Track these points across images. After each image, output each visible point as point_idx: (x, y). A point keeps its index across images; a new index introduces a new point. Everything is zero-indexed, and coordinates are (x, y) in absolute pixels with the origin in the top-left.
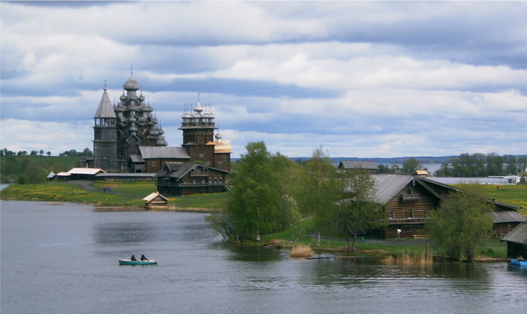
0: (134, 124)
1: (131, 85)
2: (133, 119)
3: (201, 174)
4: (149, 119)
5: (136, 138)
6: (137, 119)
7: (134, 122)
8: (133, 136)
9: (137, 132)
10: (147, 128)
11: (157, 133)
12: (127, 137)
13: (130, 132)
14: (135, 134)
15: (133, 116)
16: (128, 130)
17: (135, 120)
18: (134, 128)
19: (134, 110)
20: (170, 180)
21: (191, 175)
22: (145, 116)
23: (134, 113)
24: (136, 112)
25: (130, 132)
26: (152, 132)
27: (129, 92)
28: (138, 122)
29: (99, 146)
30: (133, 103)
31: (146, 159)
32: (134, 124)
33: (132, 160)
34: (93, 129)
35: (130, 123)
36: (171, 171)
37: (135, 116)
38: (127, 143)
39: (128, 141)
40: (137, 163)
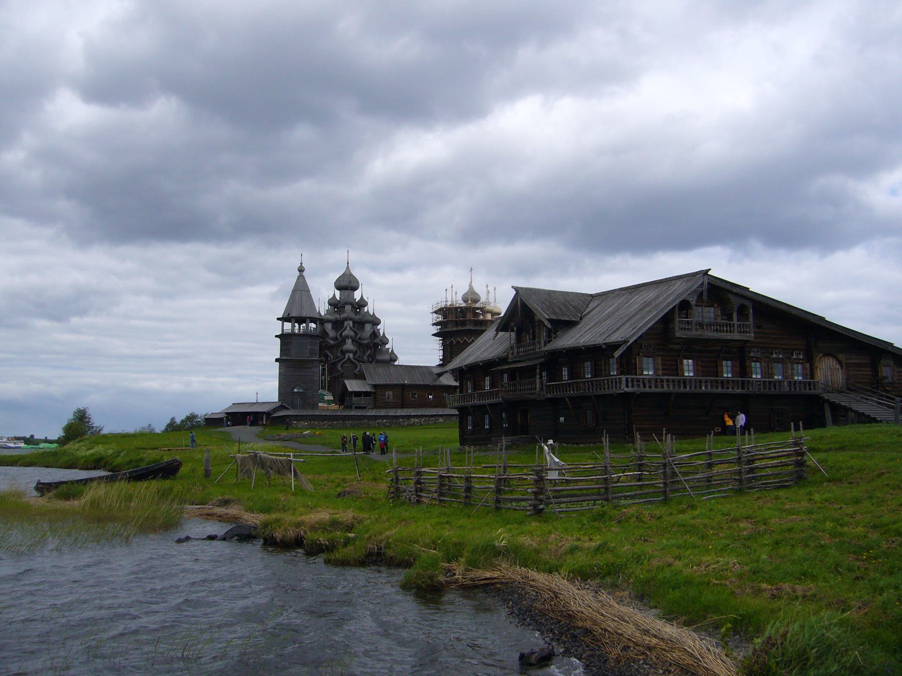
0: (349, 341)
2: (348, 332)
3: (719, 328)
5: (354, 363)
6: (356, 333)
7: (351, 337)
8: (349, 358)
9: (355, 353)
10: (371, 349)
11: (387, 357)
12: (339, 361)
13: (343, 353)
14: (351, 356)
15: (348, 328)
16: (340, 350)
17: (352, 333)
18: (349, 345)
19: (351, 319)
20: (545, 366)
21: (678, 334)
22: (368, 327)
23: (351, 323)
24: (354, 323)
25: (343, 353)
26: (379, 357)
27: (342, 291)
29: (287, 367)
30: (348, 308)
32: (349, 341)
33: (347, 389)
34: (278, 340)
35: (344, 340)
36: (550, 320)
37: (353, 329)
38: (339, 371)
39: (339, 368)
40: (358, 394)
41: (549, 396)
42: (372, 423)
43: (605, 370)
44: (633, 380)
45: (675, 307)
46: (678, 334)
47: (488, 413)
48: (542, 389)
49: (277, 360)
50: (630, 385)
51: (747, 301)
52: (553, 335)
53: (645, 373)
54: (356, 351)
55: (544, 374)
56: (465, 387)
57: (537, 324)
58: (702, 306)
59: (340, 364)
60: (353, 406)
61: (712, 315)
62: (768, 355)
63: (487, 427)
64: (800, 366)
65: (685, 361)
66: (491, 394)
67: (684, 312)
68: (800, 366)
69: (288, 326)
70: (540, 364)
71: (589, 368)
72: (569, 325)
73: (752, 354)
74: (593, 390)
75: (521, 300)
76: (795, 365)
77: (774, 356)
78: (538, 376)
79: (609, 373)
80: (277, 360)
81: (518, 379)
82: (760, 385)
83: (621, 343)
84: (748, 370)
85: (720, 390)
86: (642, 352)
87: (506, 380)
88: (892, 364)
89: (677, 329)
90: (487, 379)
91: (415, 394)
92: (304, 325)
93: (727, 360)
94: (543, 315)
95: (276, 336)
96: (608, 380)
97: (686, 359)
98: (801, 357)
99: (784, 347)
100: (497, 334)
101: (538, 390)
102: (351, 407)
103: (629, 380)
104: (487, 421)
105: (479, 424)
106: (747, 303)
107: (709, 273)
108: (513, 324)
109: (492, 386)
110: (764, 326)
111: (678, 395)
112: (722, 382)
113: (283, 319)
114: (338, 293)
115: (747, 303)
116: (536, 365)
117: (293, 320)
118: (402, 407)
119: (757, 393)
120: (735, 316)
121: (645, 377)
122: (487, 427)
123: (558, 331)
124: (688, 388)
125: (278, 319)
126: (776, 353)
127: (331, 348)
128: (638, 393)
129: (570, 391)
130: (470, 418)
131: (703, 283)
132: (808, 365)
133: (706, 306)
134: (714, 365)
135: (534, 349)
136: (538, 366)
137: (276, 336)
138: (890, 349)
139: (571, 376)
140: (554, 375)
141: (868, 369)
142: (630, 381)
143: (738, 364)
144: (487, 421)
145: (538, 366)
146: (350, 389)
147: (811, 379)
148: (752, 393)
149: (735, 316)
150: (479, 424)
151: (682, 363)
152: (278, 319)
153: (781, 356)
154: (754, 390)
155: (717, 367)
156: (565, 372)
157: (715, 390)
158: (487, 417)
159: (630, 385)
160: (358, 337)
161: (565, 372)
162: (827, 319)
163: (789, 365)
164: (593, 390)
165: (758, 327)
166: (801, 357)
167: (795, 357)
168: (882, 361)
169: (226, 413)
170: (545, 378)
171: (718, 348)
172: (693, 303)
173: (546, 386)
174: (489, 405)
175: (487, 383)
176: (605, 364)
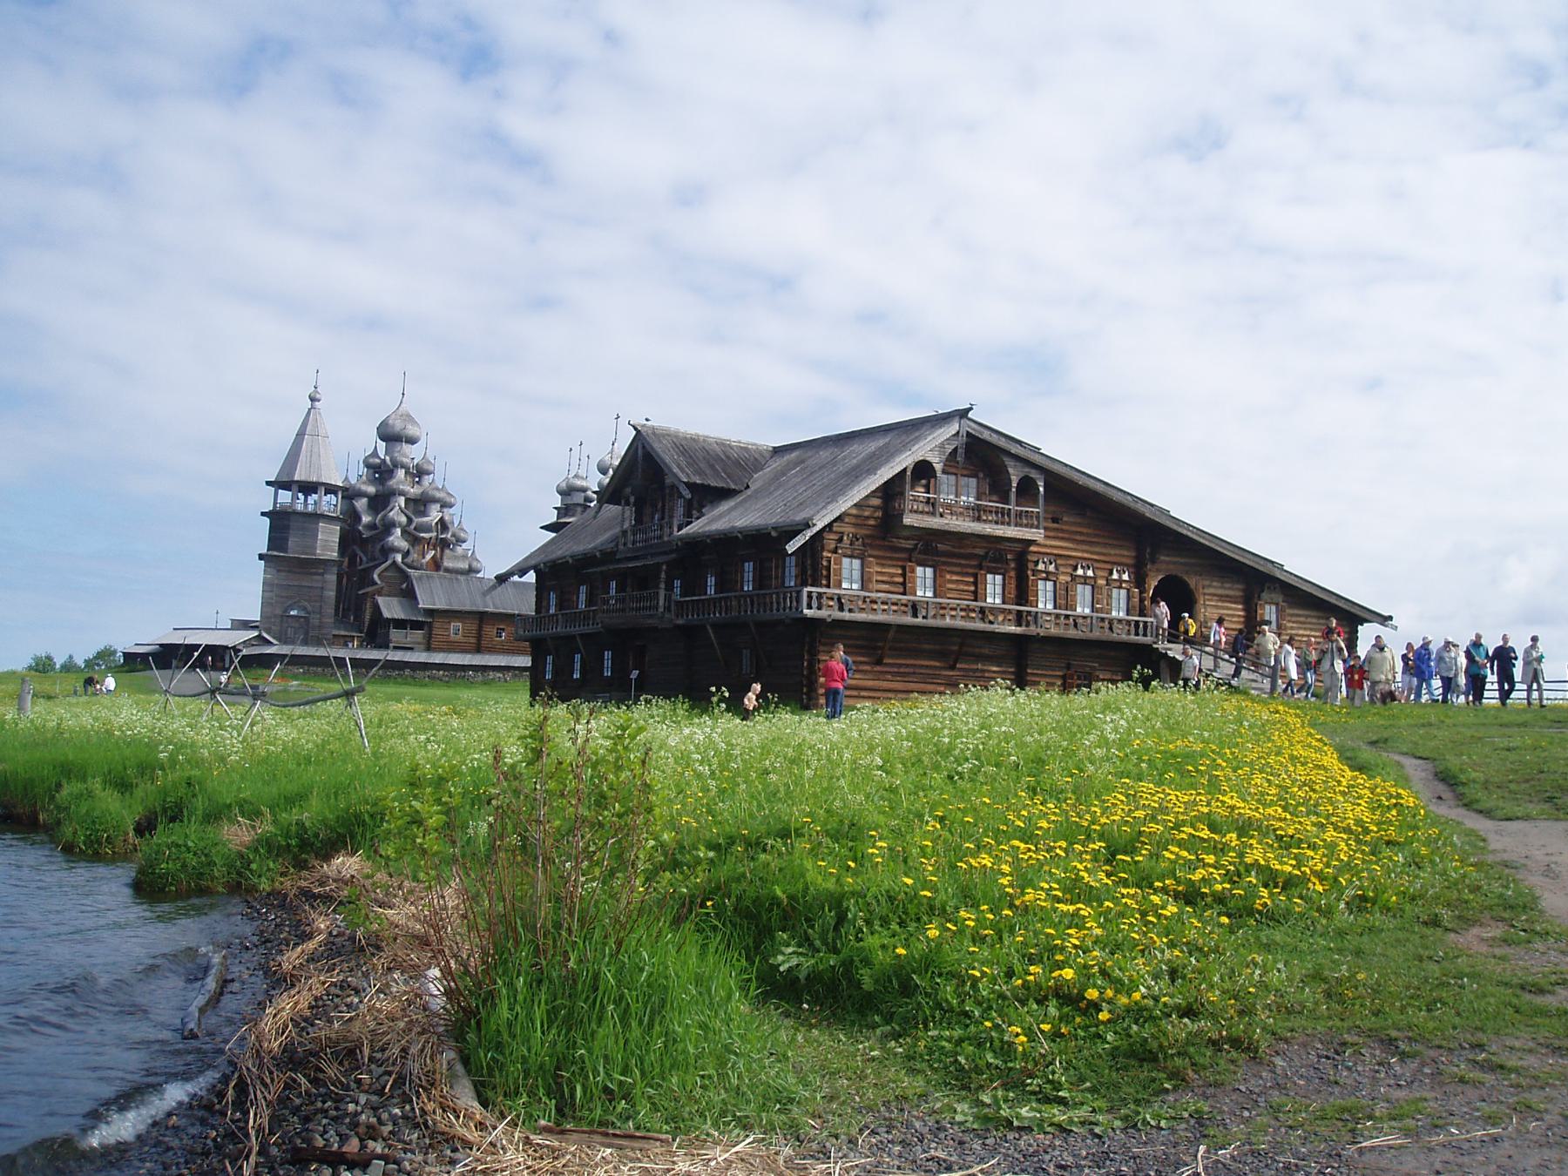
0: (398, 531)
1: (398, 425)
4: (443, 525)
6: (410, 520)
8: (394, 562)
9: (406, 554)
10: (435, 549)
11: (464, 565)
12: (376, 566)
14: (399, 558)
17: (404, 519)
19: (402, 493)
21: (908, 520)
22: (434, 515)
23: (402, 501)
24: (407, 501)
26: (447, 563)
27: (390, 443)
28: (412, 527)
29: (278, 571)
30: (401, 473)
31: (430, 612)
33: (381, 614)
34: (267, 520)
36: (691, 486)
38: (375, 583)
40: (400, 624)
41: (680, 622)
42: (419, 674)
43: (777, 577)
44: (820, 595)
45: (905, 470)
46: (908, 520)
47: (579, 652)
48: (668, 609)
49: (261, 557)
50: (815, 604)
51: (1033, 471)
52: (695, 513)
53: (845, 585)
54: (408, 551)
55: (677, 583)
56: (544, 604)
57: (667, 491)
58: (956, 474)
59: (377, 571)
60: (391, 645)
61: (973, 491)
63: (576, 676)
65: (919, 570)
66: (585, 617)
67: (924, 482)
68: (1123, 593)
69: (285, 497)
70: (668, 563)
71: (751, 574)
72: (725, 494)
74: (752, 611)
75: (644, 447)
76: (1115, 591)
77: (1080, 572)
78: (662, 586)
79: (784, 582)
80: (261, 557)
81: (628, 589)
83: (800, 528)
85: (979, 625)
86: (842, 548)
87: (613, 592)
88: (1280, 600)
90: (583, 589)
91: (503, 629)
92: (315, 496)
93: (994, 574)
94: (682, 473)
95: (263, 514)
96: (777, 594)
97: (921, 565)
100: (600, 507)
101: (661, 610)
102: (387, 647)
103: (814, 595)
104: (577, 666)
105: (562, 670)
106: (1034, 474)
107: (970, 415)
108: (628, 490)
109: (590, 602)
110: (1065, 519)
111: (902, 628)
112: (982, 611)
113: (279, 484)
114: (382, 445)
115: (1034, 474)
116: (659, 565)
117: (295, 488)
118: (478, 650)
120: (1013, 497)
121: (843, 592)
122: (576, 676)
123: (704, 506)
124: (920, 616)
125: (268, 483)
126: (1082, 567)
127: (364, 543)
128: (829, 620)
129: (715, 614)
130: (550, 659)
131: (958, 432)
133: (962, 475)
134: (972, 580)
135: (661, 537)
136: (664, 567)
137: (263, 514)
138: (1278, 574)
139: (720, 587)
140: (694, 585)
141: (1240, 607)
142: (814, 598)
144: (577, 666)
145: (664, 567)
146: (386, 614)
147: (1140, 616)
148: (1034, 634)
149: (1013, 497)
150: (562, 670)
151: (913, 571)
152: (268, 483)
155: (975, 584)
156: (711, 581)
158: (578, 657)
159: (815, 604)
160: (412, 527)
161: (711, 581)
162: (1172, 514)
164: (752, 611)
165: (1055, 520)
166: (1125, 577)
168: (1265, 595)
169: (161, 645)
170: (678, 591)
171: (981, 552)
172: (938, 467)
173: (677, 603)
174: (582, 635)
175: (583, 597)
176: (777, 567)
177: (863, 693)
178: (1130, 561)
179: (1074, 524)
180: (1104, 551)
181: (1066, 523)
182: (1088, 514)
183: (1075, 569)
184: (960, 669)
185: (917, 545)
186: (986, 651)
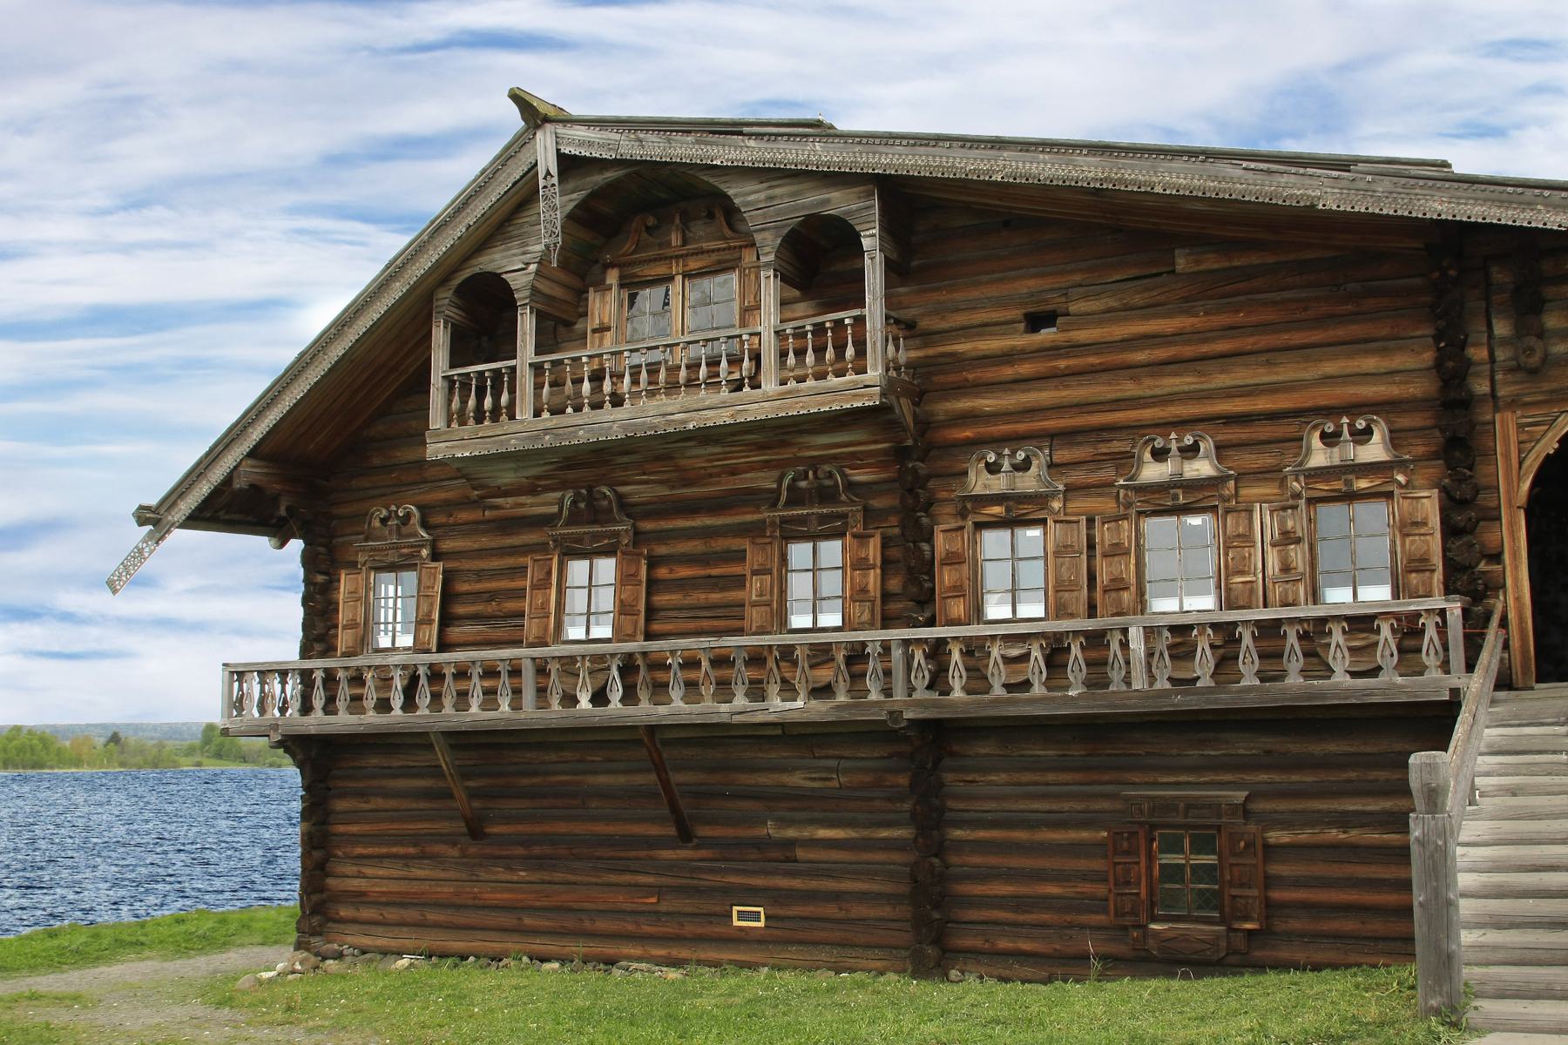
62: (1106, 473)
64: (1373, 516)
73: (980, 482)
77: (1153, 472)
82: (1025, 658)
84: (946, 577)
85: (677, 707)
86: (363, 550)
89: (436, 420)
98: (1375, 450)
99: (1051, 424)
115: (839, 202)
119: (908, 715)
132: (1429, 506)
143: (873, 550)
153: (1202, 468)
154: (899, 695)
157: (646, 710)
163: (1264, 522)
167: (1320, 457)
177: (432, 916)
178: (1419, 388)
179: (1128, 311)
180: (1263, 376)
181: (1087, 319)
182: (1182, 263)
183: (1125, 461)
184: (705, 843)
185: (561, 502)
186: (797, 780)
